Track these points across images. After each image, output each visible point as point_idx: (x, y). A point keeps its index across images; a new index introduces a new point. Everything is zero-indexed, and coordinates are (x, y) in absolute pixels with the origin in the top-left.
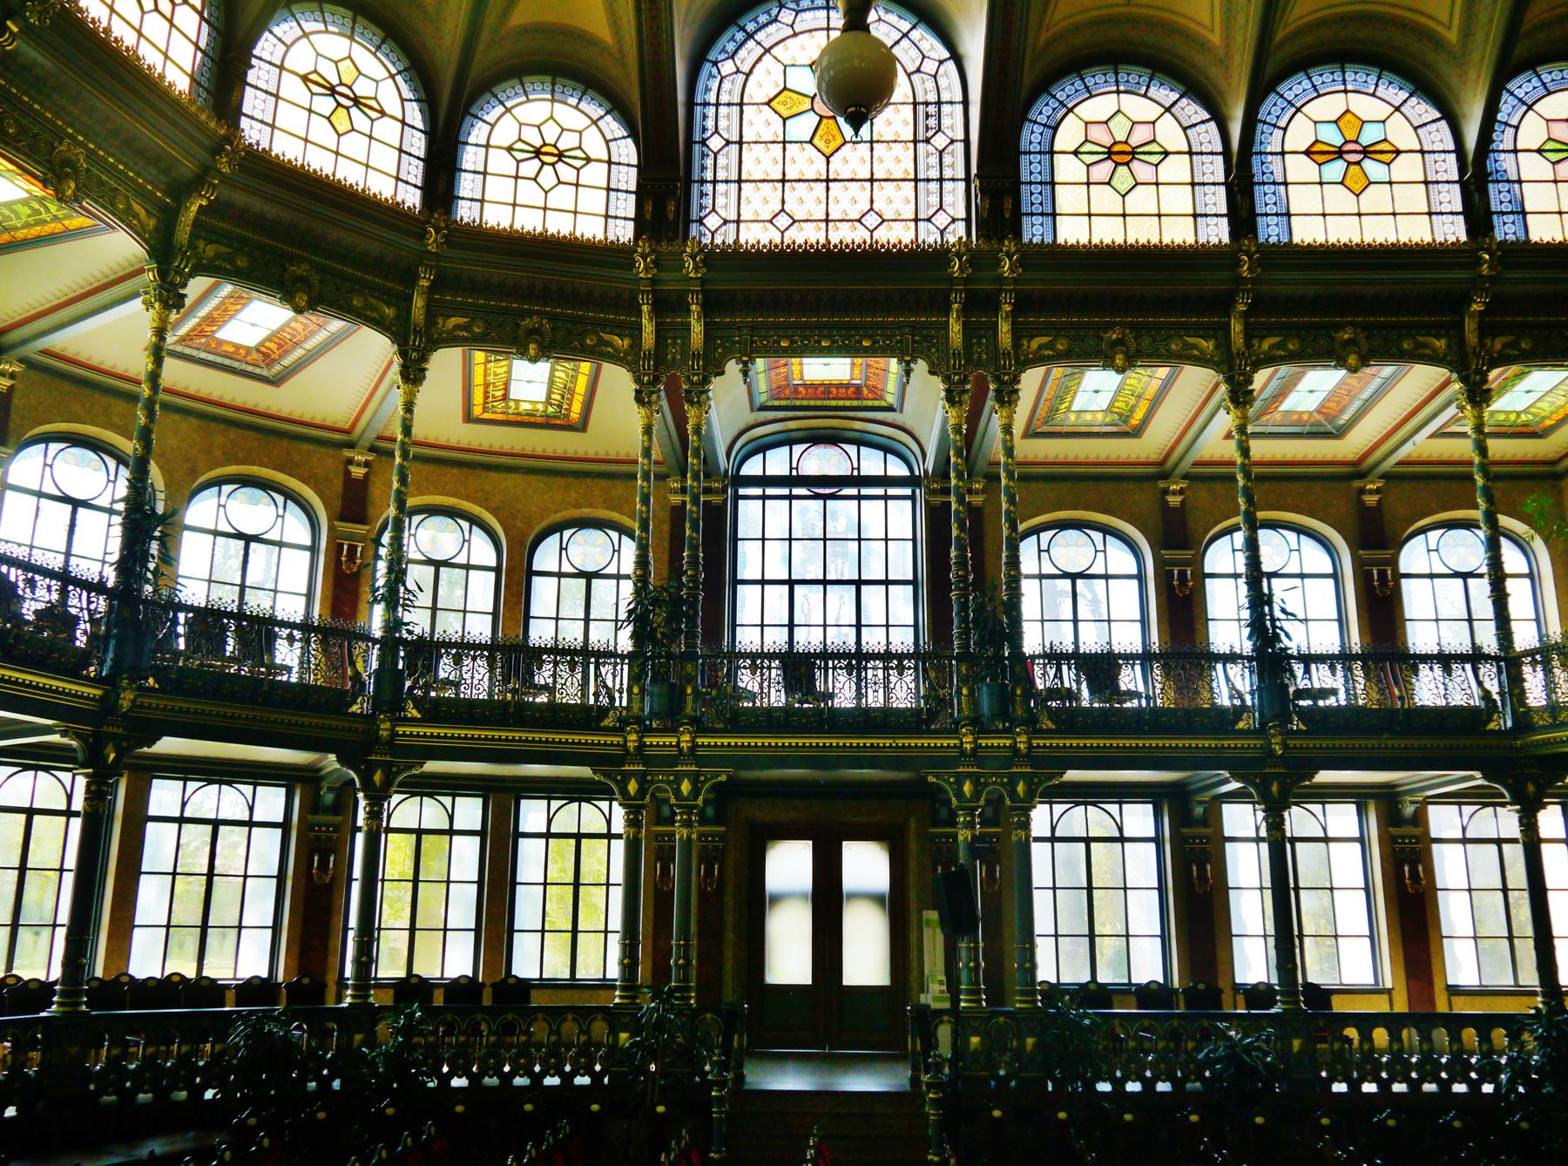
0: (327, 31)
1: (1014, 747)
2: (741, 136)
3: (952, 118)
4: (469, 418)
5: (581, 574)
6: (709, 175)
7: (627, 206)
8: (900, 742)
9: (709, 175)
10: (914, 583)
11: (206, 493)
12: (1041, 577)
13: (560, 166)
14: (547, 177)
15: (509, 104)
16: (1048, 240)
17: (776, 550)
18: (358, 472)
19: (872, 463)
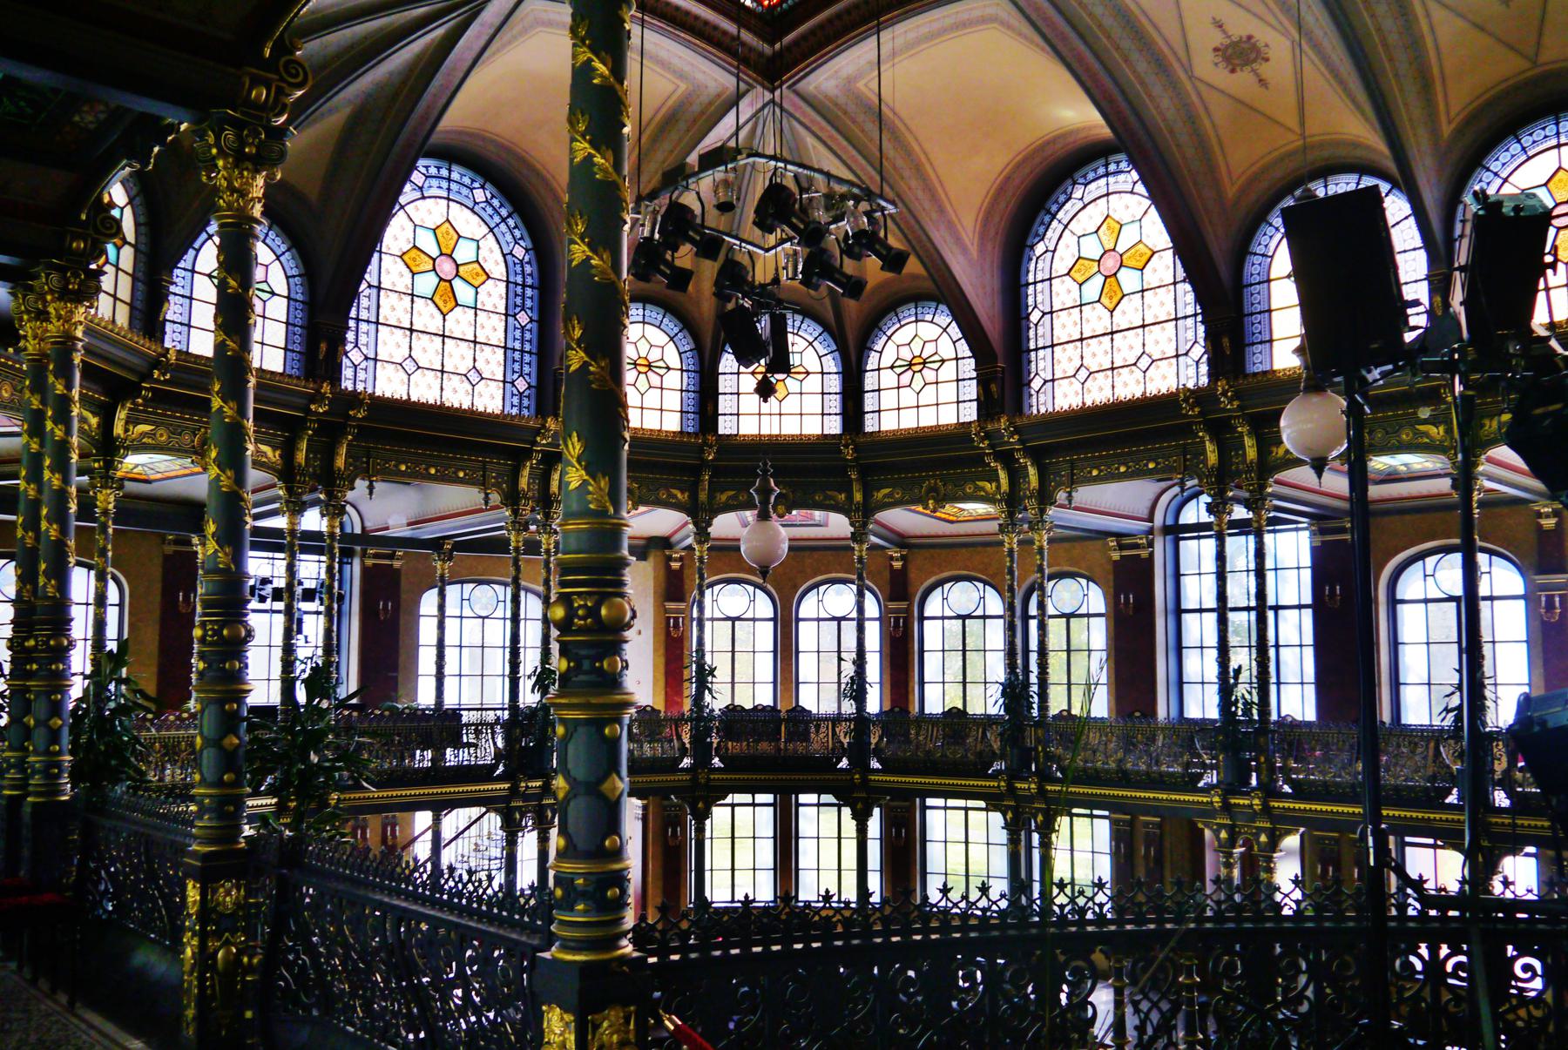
7: (971, 390)
18: (897, 565)
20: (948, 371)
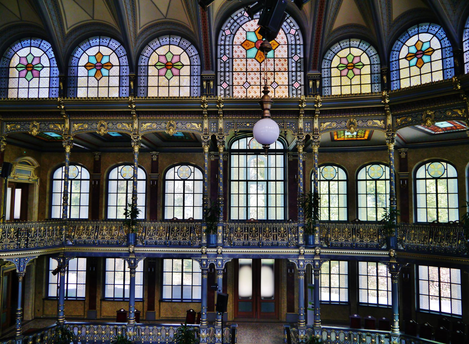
17: (242, 171)
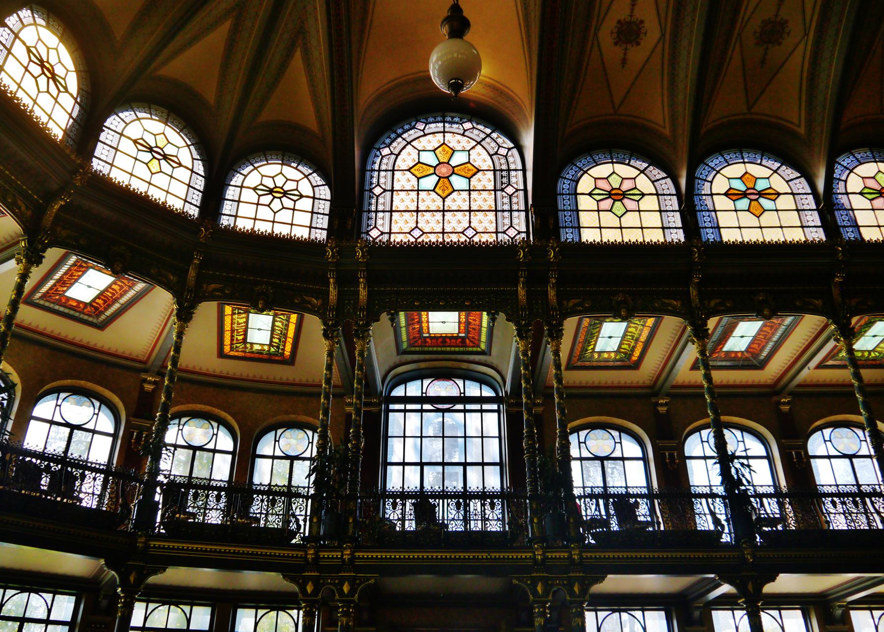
0: (151, 119)
1: (570, 558)
2: (393, 187)
3: (517, 179)
4: (221, 354)
5: (287, 457)
6: (373, 208)
7: (324, 222)
8: (493, 555)
9: (373, 208)
10: (500, 464)
11: (49, 397)
12: (581, 459)
13: (284, 199)
14: (276, 205)
15: (256, 165)
16: (576, 239)
18: (149, 387)
19: (473, 390)
20: (305, 204)
